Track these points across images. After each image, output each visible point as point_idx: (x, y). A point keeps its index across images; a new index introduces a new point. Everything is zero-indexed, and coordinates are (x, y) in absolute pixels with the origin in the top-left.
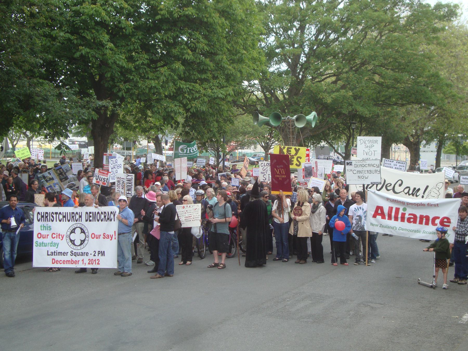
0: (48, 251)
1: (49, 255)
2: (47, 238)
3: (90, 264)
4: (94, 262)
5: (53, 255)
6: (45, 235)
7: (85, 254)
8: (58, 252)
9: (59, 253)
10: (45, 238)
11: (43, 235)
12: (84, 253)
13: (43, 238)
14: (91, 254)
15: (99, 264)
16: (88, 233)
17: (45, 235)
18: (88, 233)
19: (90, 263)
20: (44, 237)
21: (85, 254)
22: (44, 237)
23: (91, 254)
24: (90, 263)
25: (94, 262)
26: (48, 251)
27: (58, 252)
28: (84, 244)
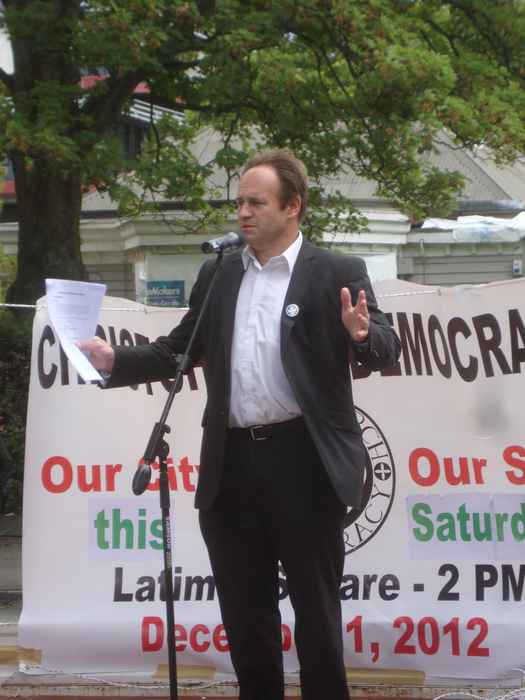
0: (119, 572)
1: (128, 598)
2: (111, 487)
3: (411, 650)
4: (446, 640)
5: (151, 597)
6: (96, 469)
7: (375, 587)
8: (183, 576)
9: (190, 581)
10: (96, 486)
11: (82, 470)
12: (369, 580)
13: (84, 487)
14: (419, 588)
15: (485, 652)
16: (382, 450)
17: (96, 469)
18: (382, 450)
19: (414, 640)
20: (89, 480)
21: (375, 587)
22: (89, 480)
23: (419, 588)
24: (414, 640)
25: (446, 640)
26: (119, 572)
27: (183, 576)
28: (361, 520)
